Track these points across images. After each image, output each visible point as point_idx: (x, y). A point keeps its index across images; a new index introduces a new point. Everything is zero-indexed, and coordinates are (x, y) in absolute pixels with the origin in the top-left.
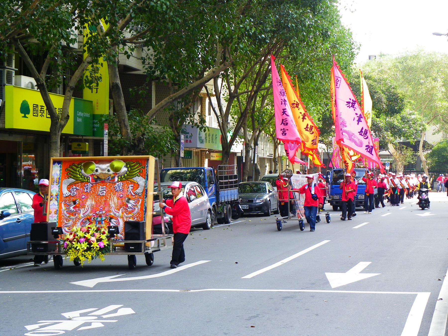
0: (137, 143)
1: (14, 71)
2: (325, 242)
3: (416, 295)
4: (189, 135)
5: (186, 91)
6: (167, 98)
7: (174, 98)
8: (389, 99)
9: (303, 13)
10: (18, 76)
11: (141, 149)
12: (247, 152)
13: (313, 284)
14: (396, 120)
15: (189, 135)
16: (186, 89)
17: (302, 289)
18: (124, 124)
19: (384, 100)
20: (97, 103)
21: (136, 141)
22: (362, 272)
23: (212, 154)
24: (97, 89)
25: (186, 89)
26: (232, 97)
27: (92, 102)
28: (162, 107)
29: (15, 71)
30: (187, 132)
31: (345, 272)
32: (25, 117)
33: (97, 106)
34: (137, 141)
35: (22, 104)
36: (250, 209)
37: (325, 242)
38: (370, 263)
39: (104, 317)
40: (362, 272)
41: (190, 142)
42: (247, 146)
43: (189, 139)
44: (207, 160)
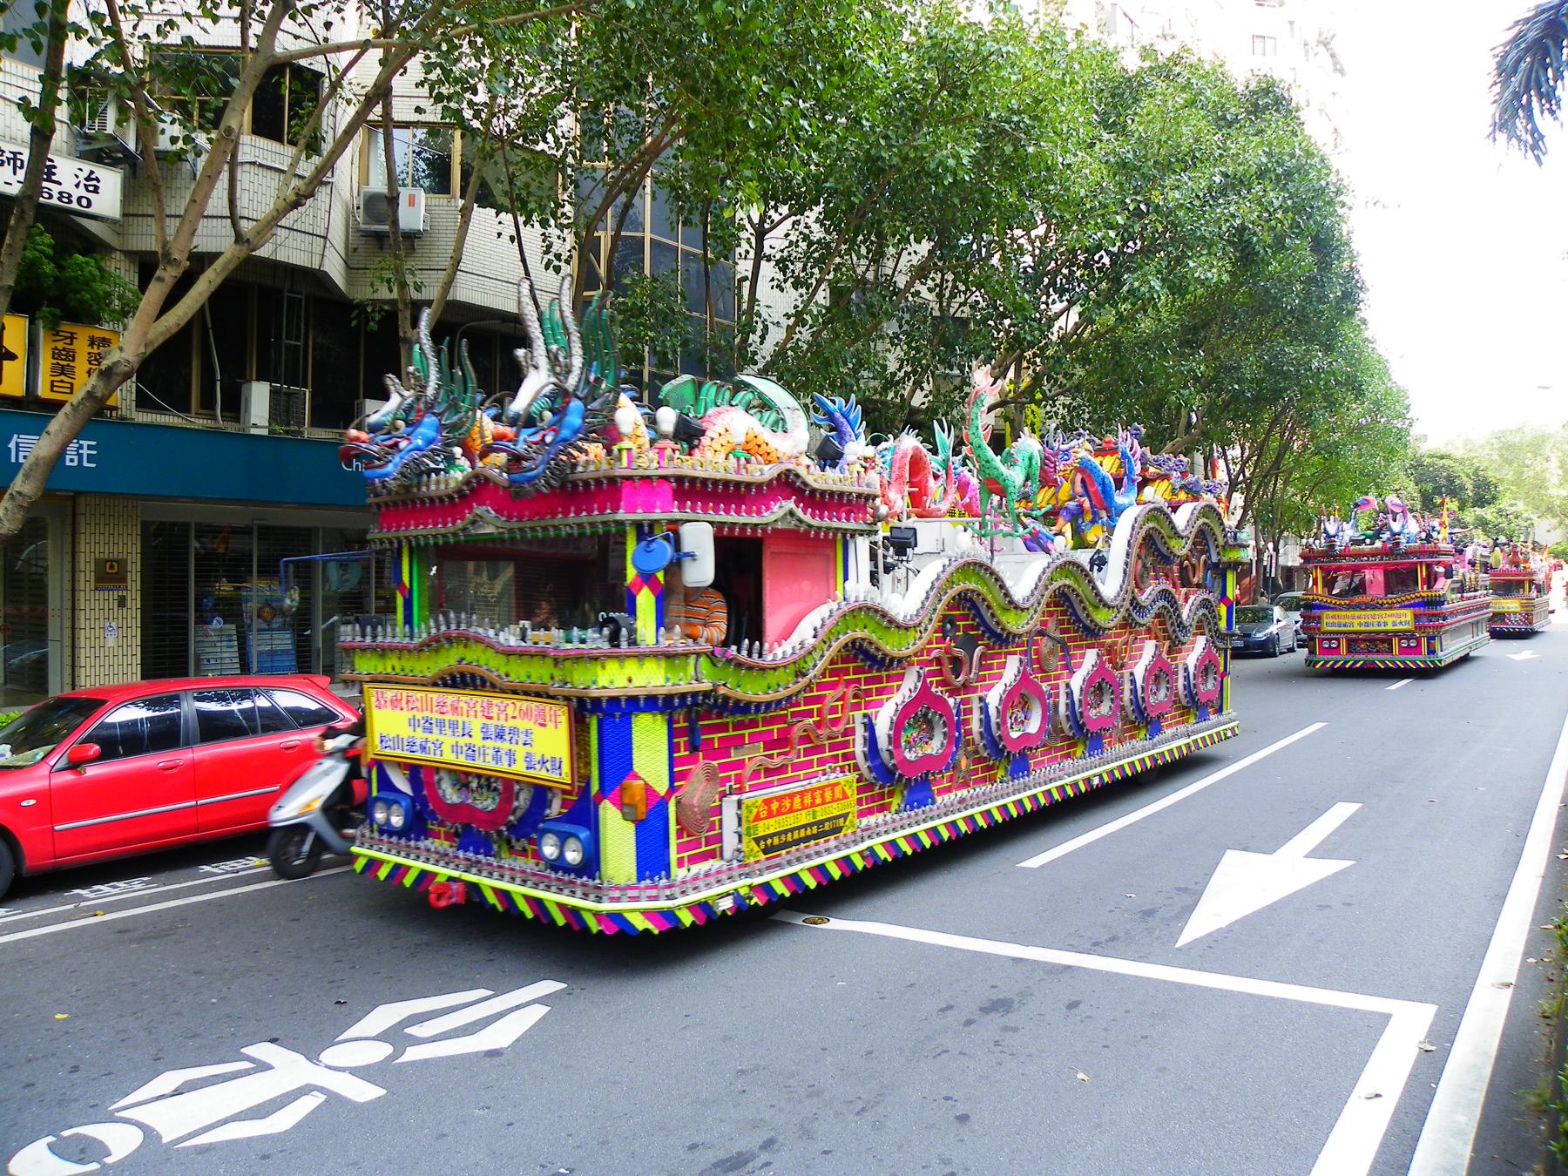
2: (1318, 726)
3: (1386, 1018)
8: (1477, 486)
9: (1307, 350)
12: (1260, 561)
13: (1149, 913)
14: (1488, 513)
17: (1096, 947)
19: (1469, 486)
22: (1316, 853)
26: (1233, 486)
31: (1270, 850)
36: (1247, 647)
37: (1318, 726)
38: (1357, 806)
39: (413, 1054)
40: (1316, 853)
42: (1260, 552)
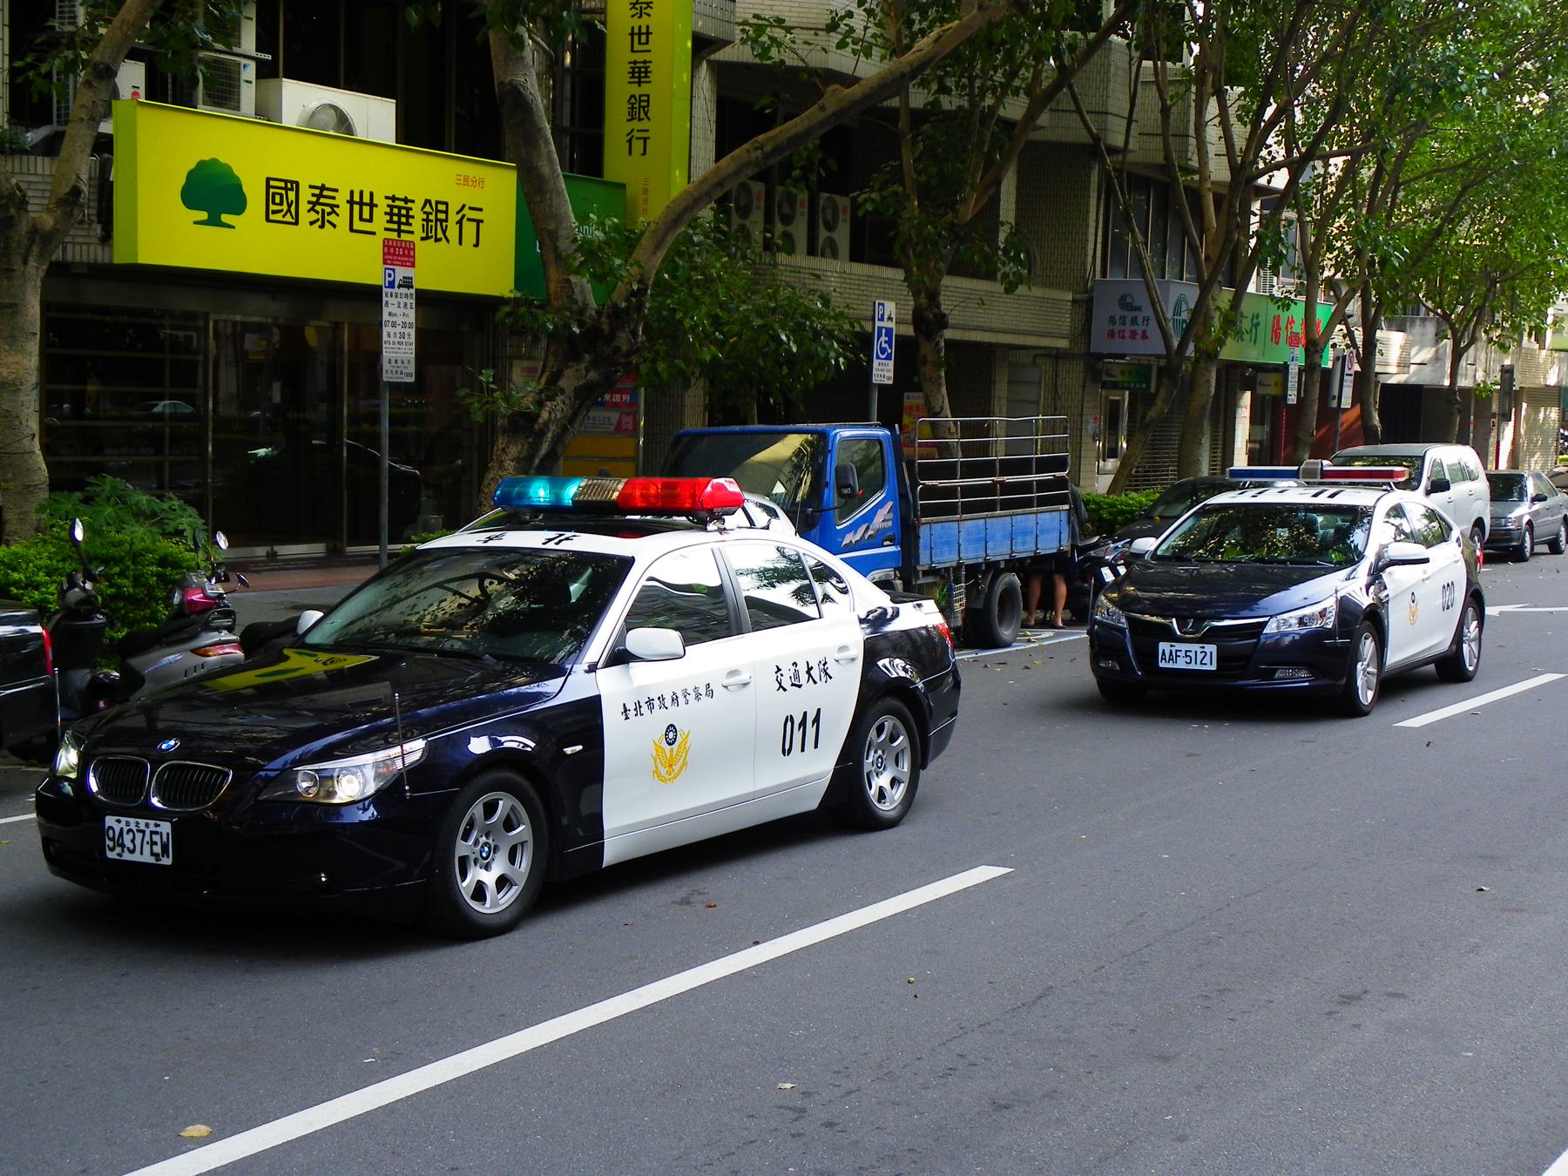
0: (606, 328)
1: (252, 65)
4: (1140, 316)
5: (822, 115)
6: (745, 146)
7: (768, 148)
10: (272, 82)
11: (618, 349)
15: (1140, 316)
16: (823, 109)
18: (556, 249)
20: (646, 191)
21: (604, 319)
23: (1261, 377)
24: (645, 139)
25: (823, 109)
27: (623, 186)
28: (720, 184)
29: (260, 64)
30: (1137, 304)
32: (213, 221)
33: (646, 201)
34: (609, 317)
35: (191, 174)
41: (1144, 336)
43: (1139, 329)
44: (1248, 395)
